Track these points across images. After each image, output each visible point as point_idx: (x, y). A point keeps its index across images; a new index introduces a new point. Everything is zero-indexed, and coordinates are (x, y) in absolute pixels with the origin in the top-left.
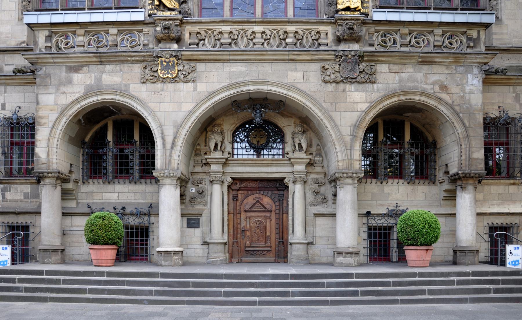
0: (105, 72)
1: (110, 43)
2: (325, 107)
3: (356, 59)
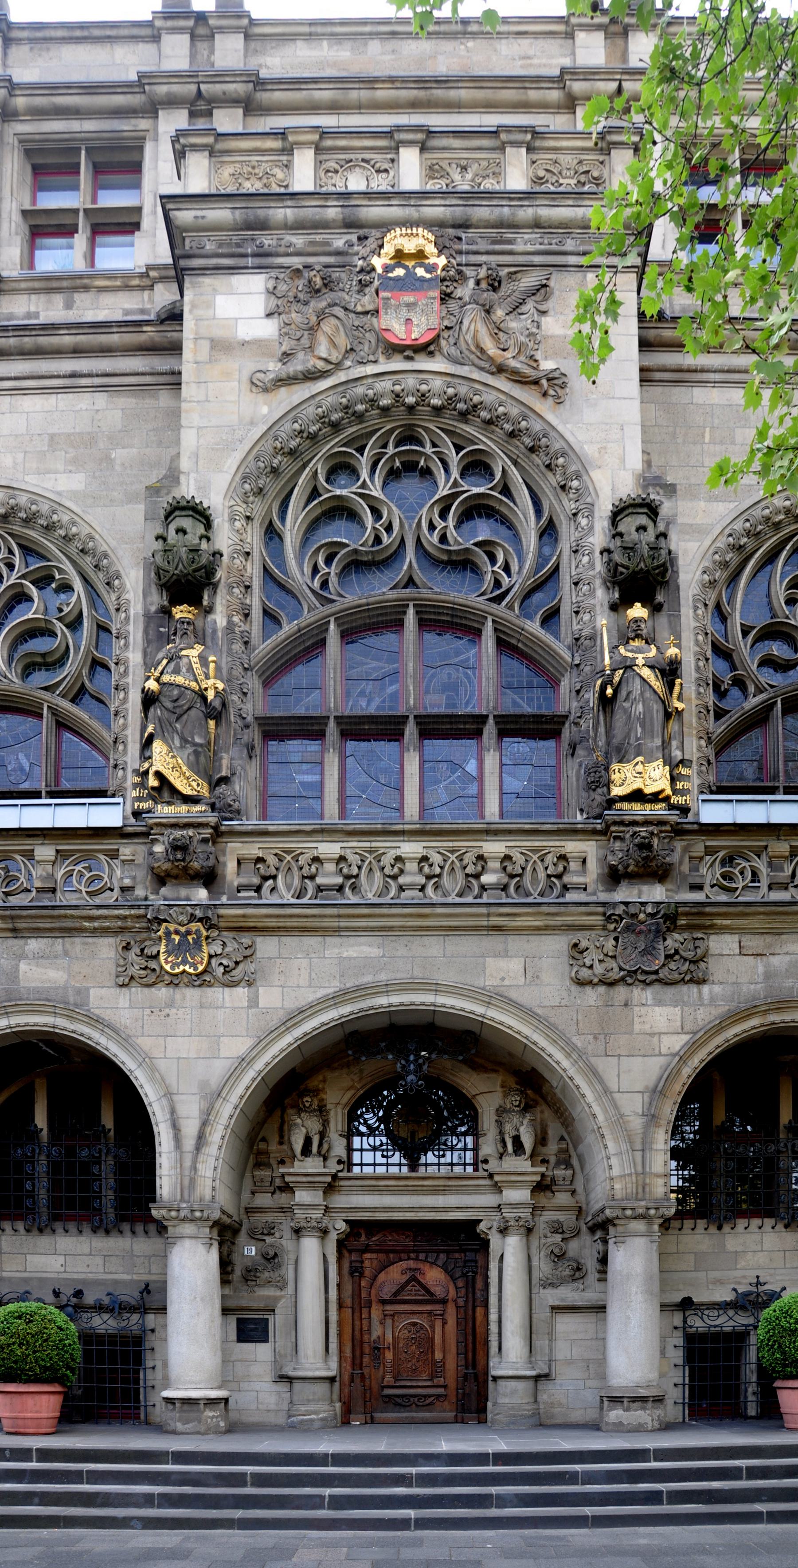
0: (27, 957)
1: (38, 884)
2: (579, 1045)
3: (658, 924)
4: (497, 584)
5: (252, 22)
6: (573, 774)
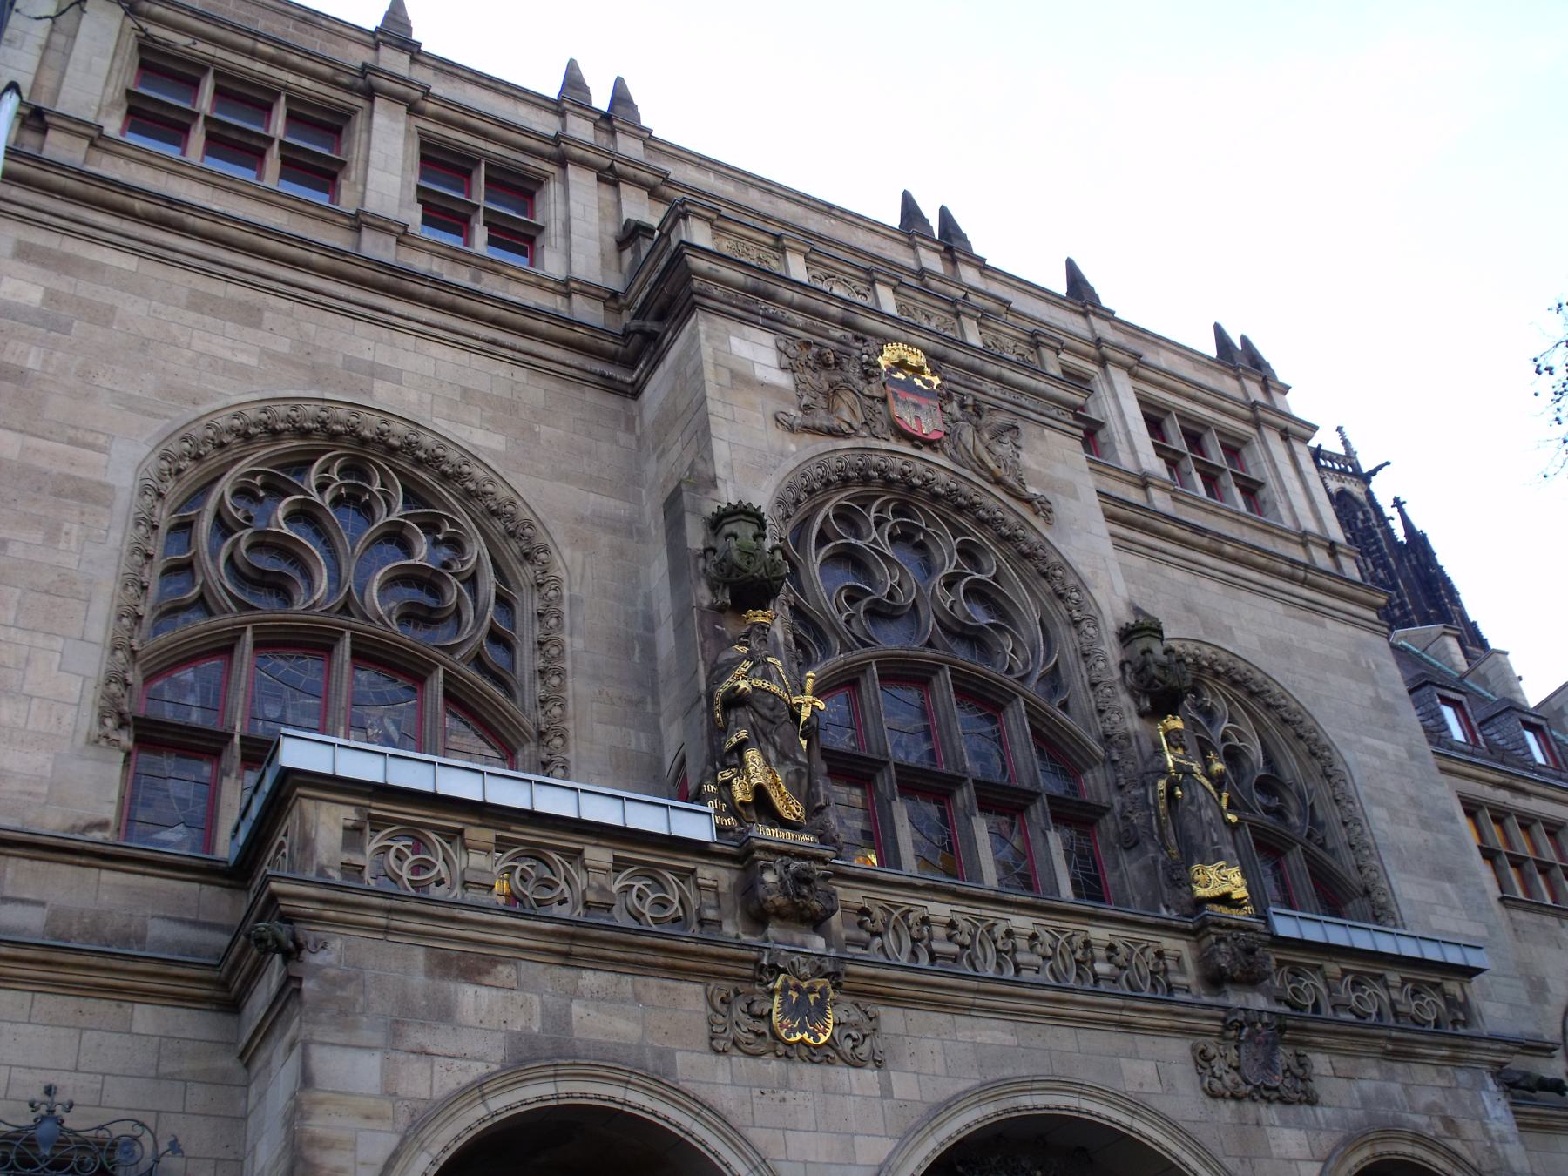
0: (582, 997)
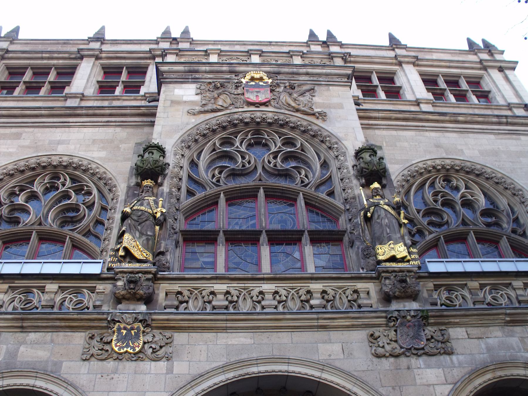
1: (43, 303)
2: (384, 393)
3: (419, 321)
4: (302, 182)
5: (193, 40)
6: (354, 256)
